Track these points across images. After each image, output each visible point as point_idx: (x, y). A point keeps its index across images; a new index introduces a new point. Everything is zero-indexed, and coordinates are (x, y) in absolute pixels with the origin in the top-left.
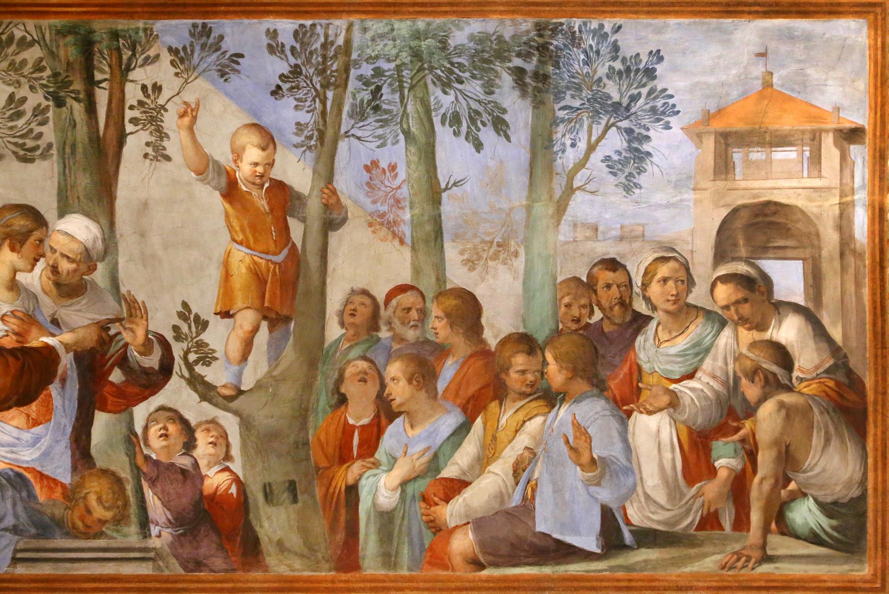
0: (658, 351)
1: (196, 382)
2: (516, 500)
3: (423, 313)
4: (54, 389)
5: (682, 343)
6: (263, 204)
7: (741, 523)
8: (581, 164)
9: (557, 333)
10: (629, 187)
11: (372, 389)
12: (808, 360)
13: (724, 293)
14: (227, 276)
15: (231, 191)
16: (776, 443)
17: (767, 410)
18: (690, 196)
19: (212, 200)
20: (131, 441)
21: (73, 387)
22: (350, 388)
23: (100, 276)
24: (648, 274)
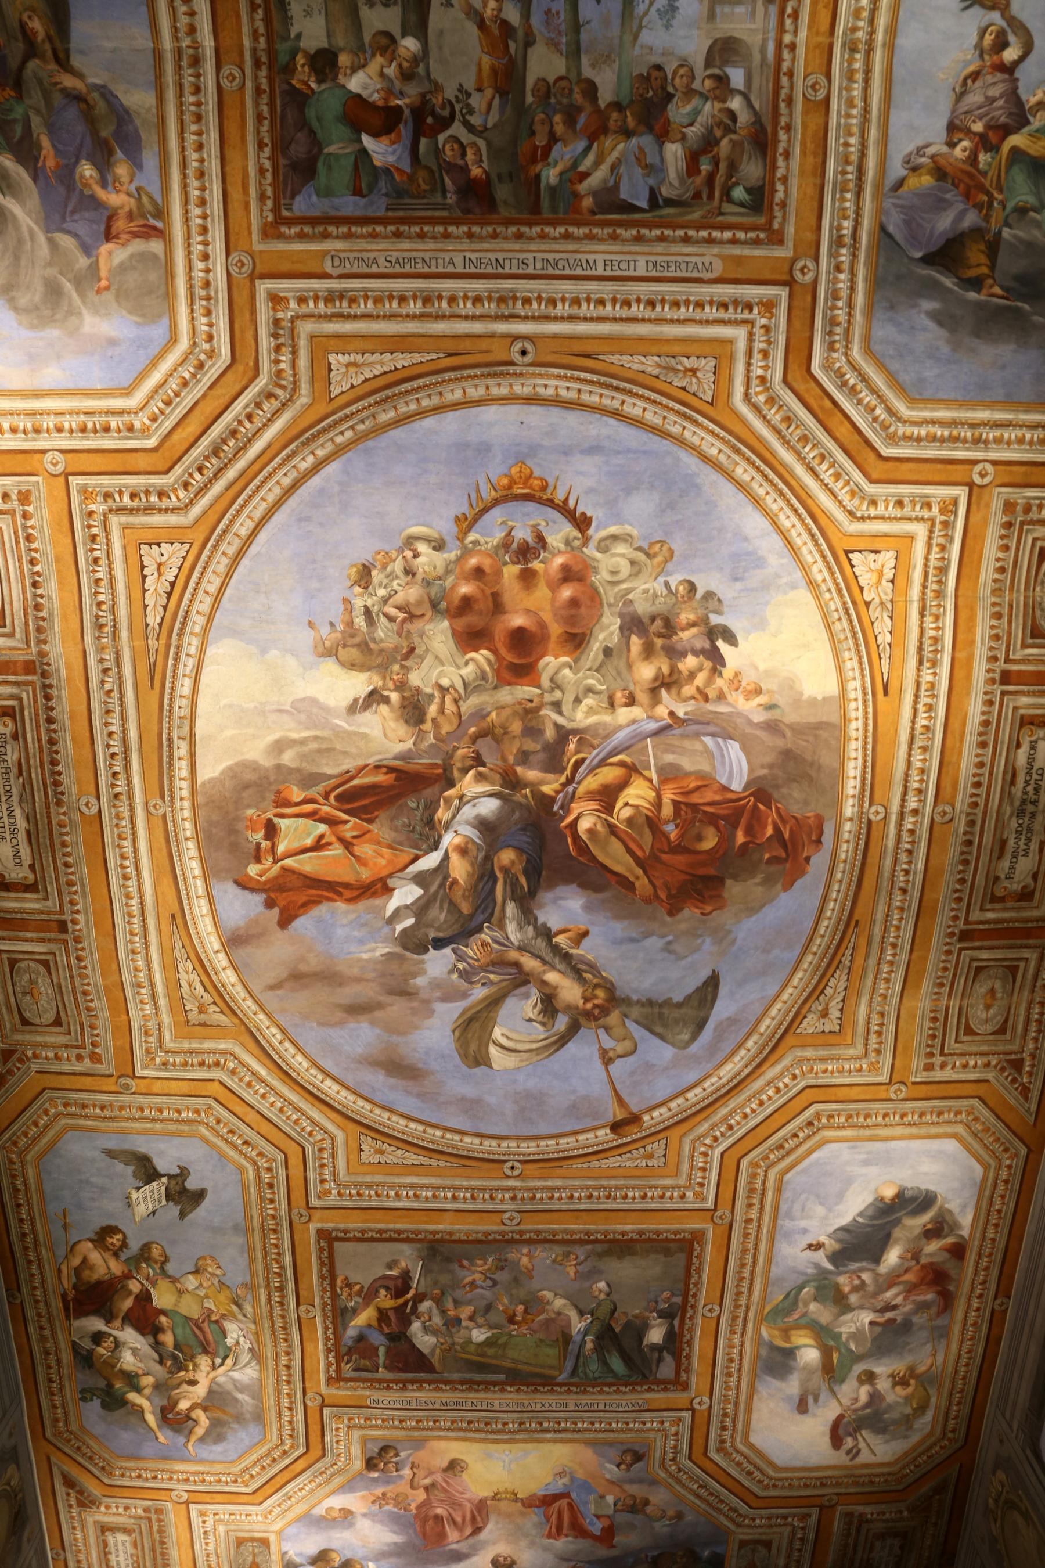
0: (678, 112)
1: (466, 124)
2: (611, 183)
3: (571, 91)
4: (401, 126)
5: (689, 108)
6: (496, 32)
7: (711, 197)
8: (646, 13)
9: (632, 102)
10: (668, 27)
11: (547, 128)
12: (744, 118)
13: (708, 83)
14: (480, 70)
15: (481, 25)
16: (728, 158)
17: (725, 142)
18: (695, 32)
19: (472, 29)
20: (437, 152)
21: (410, 125)
22: (537, 127)
23: (421, 69)
24: (675, 73)
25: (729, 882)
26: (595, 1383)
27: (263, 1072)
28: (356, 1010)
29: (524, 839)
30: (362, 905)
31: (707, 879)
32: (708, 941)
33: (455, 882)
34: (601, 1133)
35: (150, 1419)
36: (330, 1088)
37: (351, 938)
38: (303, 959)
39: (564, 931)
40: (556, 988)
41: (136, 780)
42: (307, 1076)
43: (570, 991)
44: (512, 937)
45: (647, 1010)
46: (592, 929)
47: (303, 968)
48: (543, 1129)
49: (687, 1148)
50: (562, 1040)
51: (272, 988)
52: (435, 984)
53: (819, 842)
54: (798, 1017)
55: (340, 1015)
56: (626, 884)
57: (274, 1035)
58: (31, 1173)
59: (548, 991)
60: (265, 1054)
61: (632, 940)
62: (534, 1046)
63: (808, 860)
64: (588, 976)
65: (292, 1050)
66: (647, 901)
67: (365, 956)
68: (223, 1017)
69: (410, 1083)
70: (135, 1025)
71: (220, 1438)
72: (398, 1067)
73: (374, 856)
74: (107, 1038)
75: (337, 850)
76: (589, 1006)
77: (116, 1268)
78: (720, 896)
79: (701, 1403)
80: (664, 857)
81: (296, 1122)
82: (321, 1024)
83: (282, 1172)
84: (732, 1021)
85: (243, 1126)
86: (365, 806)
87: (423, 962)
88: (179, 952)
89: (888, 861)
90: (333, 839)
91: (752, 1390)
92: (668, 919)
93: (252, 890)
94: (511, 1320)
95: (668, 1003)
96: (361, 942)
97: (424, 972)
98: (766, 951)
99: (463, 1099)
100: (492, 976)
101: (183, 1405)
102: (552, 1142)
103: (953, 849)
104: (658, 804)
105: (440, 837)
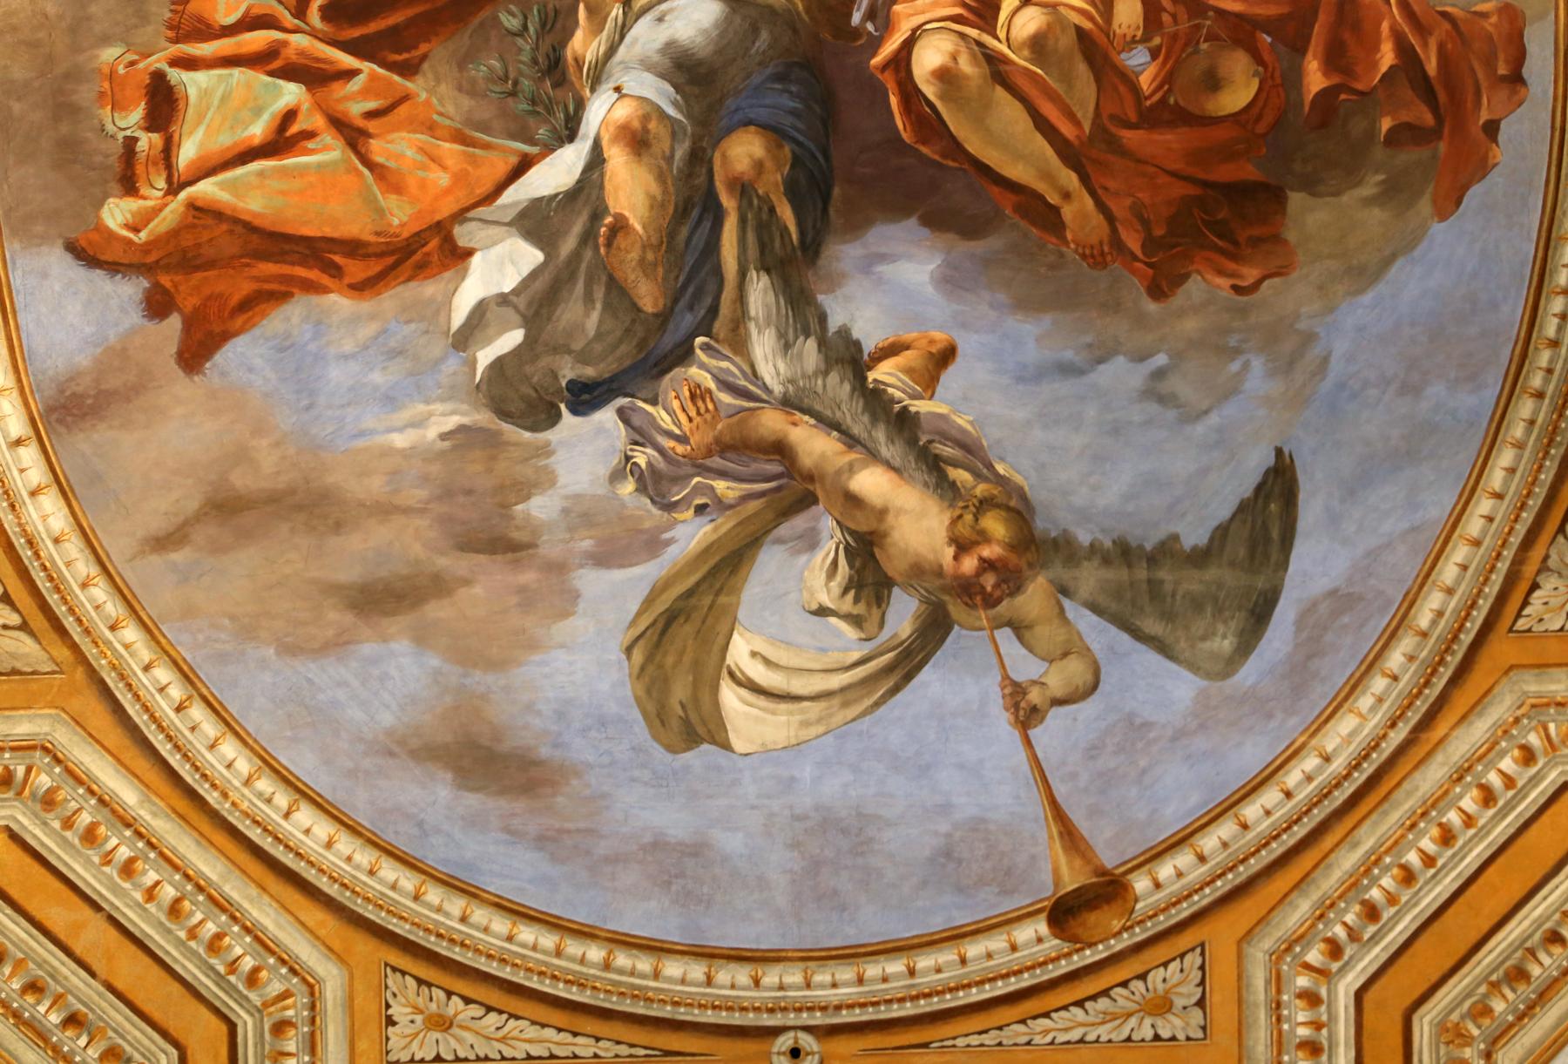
25: (1296, 199)
27: (128, 795)
28: (382, 599)
29: (782, 102)
30: (392, 299)
31: (1238, 192)
32: (1257, 364)
33: (620, 226)
34: (1024, 933)
36: (308, 831)
37: (366, 390)
38: (242, 455)
39: (892, 350)
40: (882, 513)
42: (247, 799)
43: (919, 525)
44: (766, 372)
45: (1118, 574)
46: (967, 344)
47: (242, 480)
48: (872, 925)
49: (1258, 978)
50: (907, 663)
51: (162, 543)
52: (580, 515)
53: (1516, 79)
54: (1516, 587)
55: (336, 616)
57: (160, 686)
59: (863, 527)
61: (1067, 370)
62: (836, 681)
63: (1492, 129)
64: (960, 476)
65: (210, 728)
66: (1096, 258)
67: (400, 440)
68: (26, 645)
69: (520, 805)
72: (491, 762)
73: (423, 162)
75: (328, 152)
76: (969, 564)
78: (1277, 239)
80: (1130, 137)
81: (215, 944)
82: (290, 649)
84: (1342, 600)
85: (66, 968)
86: (394, 31)
87: (546, 450)
90: (319, 122)
92: (1152, 307)
93: (113, 268)
95: (1167, 550)
96: (390, 400)
97: (546, 480)
98: (1410, 390)
99: (658, 845)
100: (720, 485)
102: (896, 966)
105: (580, 105)
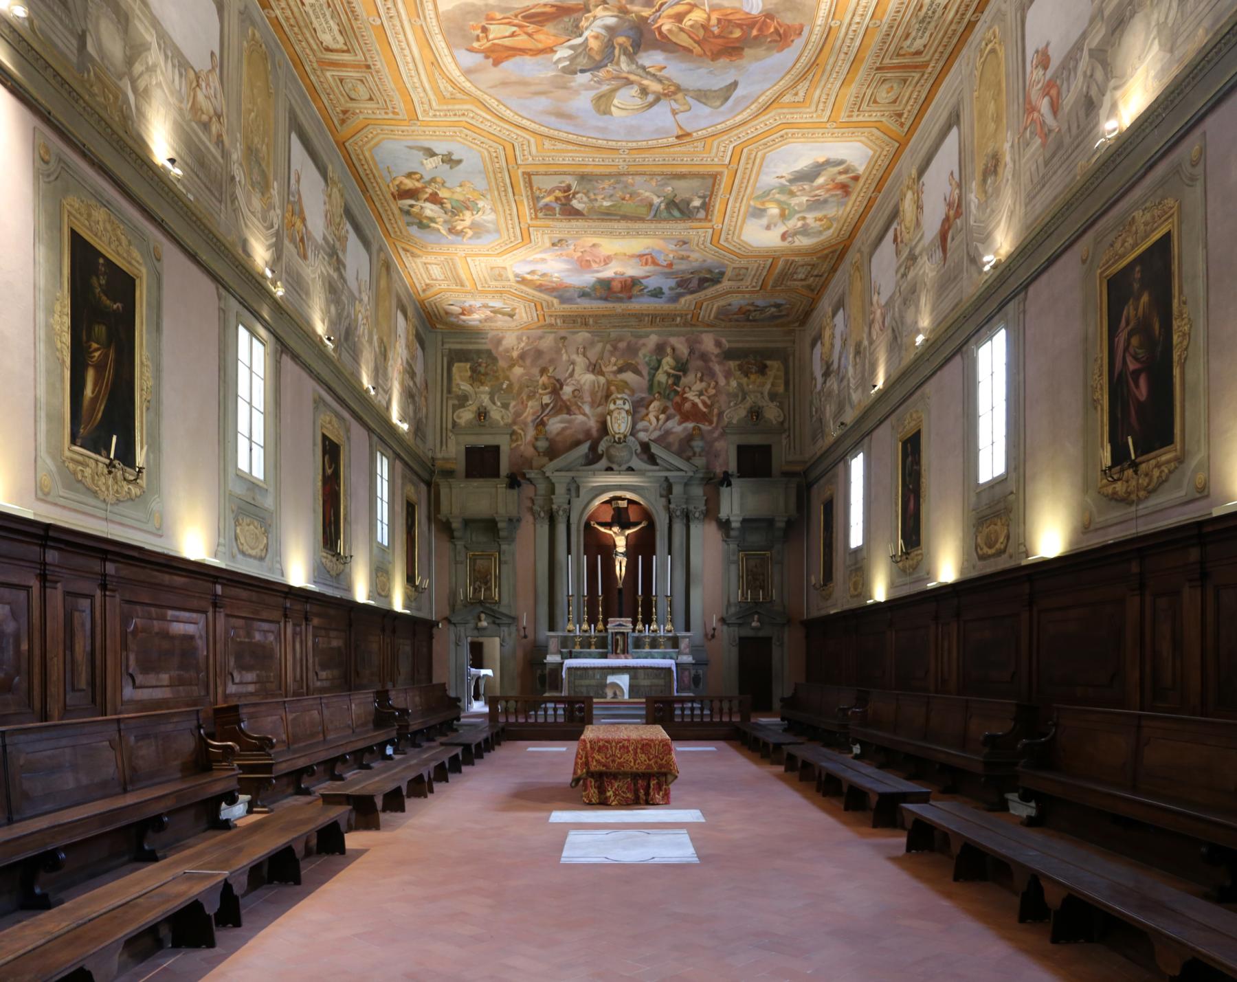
26: (665, 220)
27: (489, 117)
29: (631, 33)
30: (540, 58)
31: (735, 49)
35: (443, 232)
36: (525, 123)
41: (402, 11)
43: (655, 87)
48: (639, 138)
50: (651, 105)
52: (581, 85)
54: (781, 95)
56: (688, 50)
58: (367, 154)
60: (488, 110)
70: (415, 100)
71: (479, 238)
74: (401, 106)
75: (525, 37)
77: (418, 185)
79: (718, 226)
83: (502, 153)
84: (744, 97)
88: (437, 74)
89: (839, 43)
91: (744, 222)
94: (623, 199)
101: (459, 228)
103: (878, 37)
104: (709, 19)
